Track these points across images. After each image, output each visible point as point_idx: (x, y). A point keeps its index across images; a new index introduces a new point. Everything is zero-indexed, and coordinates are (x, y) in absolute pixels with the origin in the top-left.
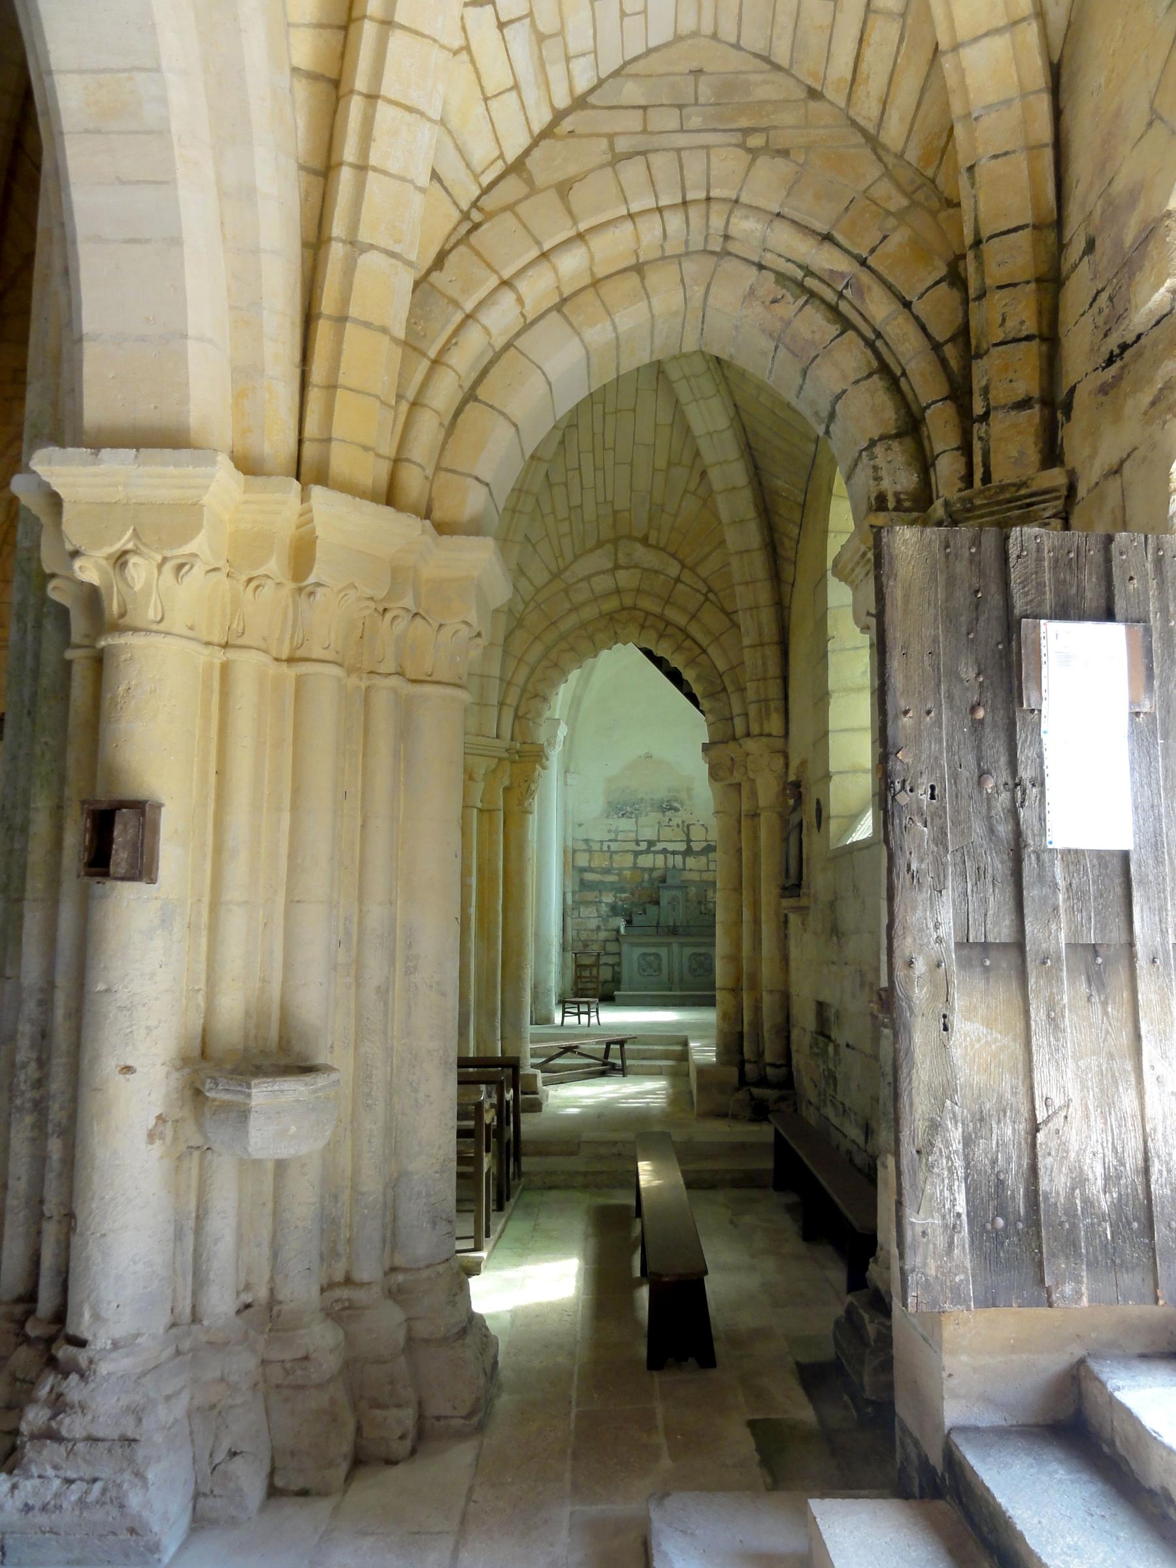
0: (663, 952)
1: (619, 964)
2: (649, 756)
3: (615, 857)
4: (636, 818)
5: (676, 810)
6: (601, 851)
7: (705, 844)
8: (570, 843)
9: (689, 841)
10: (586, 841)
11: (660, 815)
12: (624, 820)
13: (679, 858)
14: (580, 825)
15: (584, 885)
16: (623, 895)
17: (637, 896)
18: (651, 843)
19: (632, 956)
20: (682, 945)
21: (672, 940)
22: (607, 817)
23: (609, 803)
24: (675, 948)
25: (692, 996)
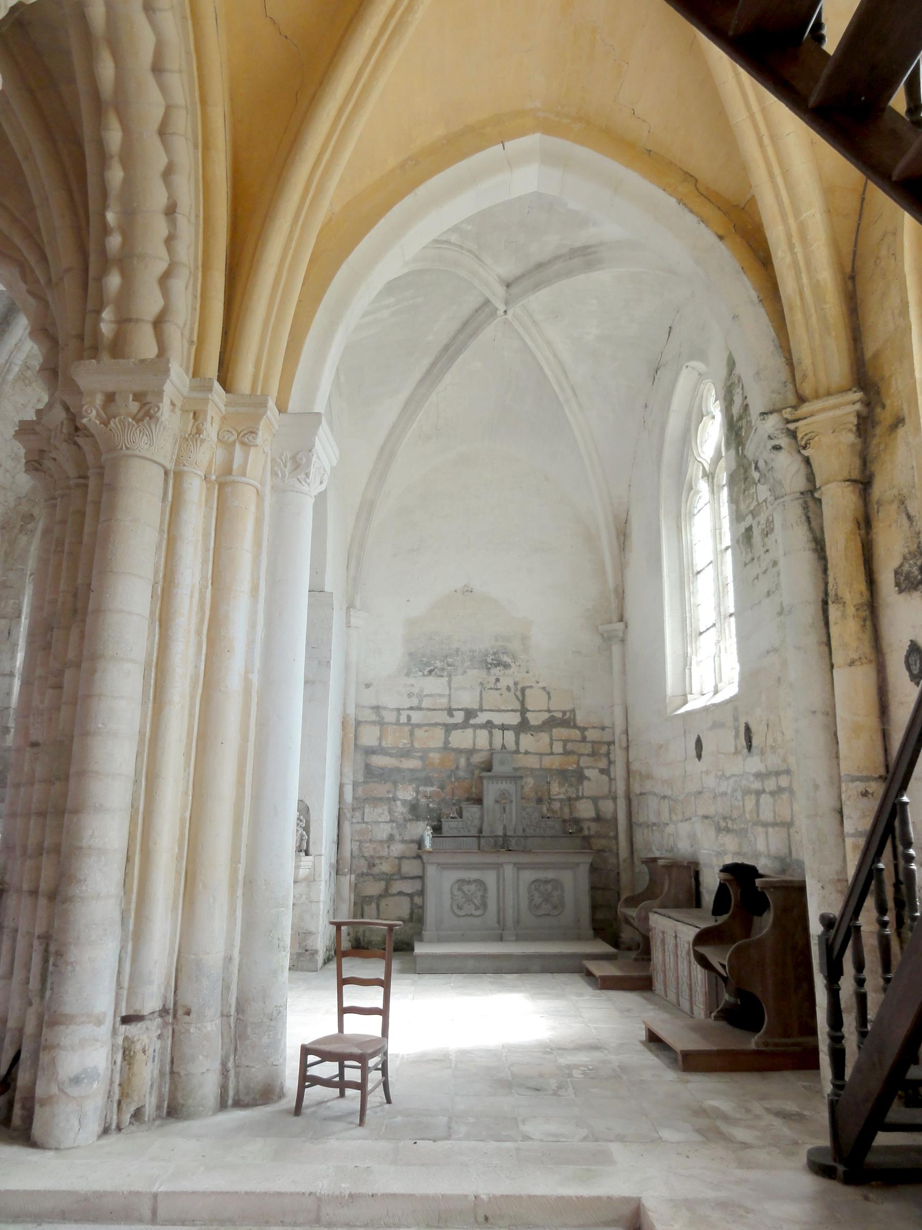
0: (490, 878)
1: (422, 893)
2: (468, 591)
3: (419, 733)
4: (450, 676)
5: (506, 666)
6: (398, 723)
7: (546, 716)
8: (351, 711)
9: (523, 711)
10: (377, 709)
11: (483, 673)
12: (431, 679)
13: (510, 736)
14: (368, 686)
15: (370, 772)
16: (429, 789)
17: (448, 789)
18: (470, 714)
19: (442, 884)
20: (519, 867)
21: (504, 858)
22: (407, 675)
23: (410, 654)
24: (509, 871)
25: (542, 956)
